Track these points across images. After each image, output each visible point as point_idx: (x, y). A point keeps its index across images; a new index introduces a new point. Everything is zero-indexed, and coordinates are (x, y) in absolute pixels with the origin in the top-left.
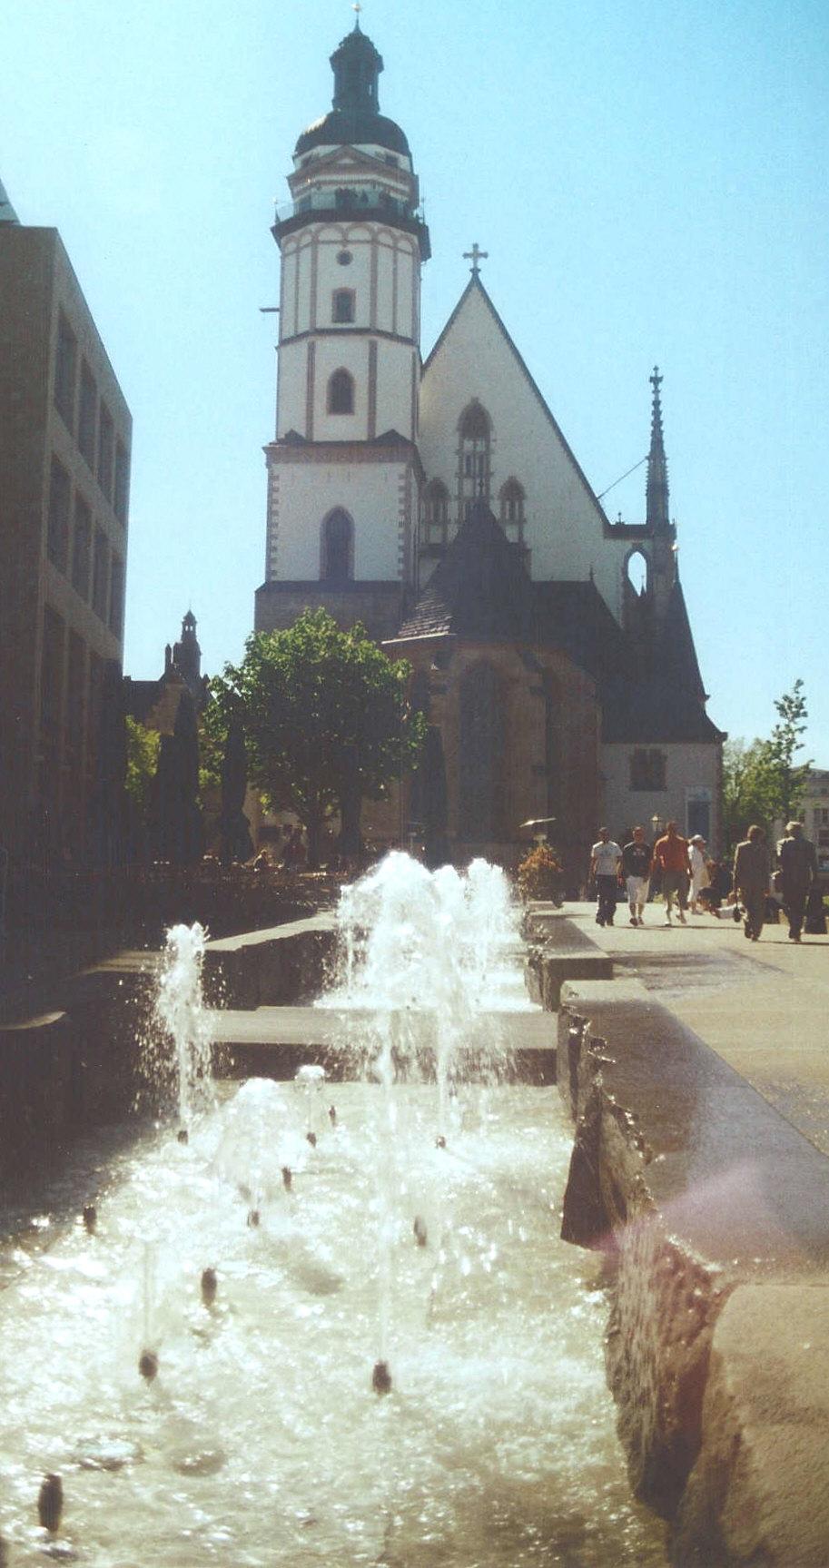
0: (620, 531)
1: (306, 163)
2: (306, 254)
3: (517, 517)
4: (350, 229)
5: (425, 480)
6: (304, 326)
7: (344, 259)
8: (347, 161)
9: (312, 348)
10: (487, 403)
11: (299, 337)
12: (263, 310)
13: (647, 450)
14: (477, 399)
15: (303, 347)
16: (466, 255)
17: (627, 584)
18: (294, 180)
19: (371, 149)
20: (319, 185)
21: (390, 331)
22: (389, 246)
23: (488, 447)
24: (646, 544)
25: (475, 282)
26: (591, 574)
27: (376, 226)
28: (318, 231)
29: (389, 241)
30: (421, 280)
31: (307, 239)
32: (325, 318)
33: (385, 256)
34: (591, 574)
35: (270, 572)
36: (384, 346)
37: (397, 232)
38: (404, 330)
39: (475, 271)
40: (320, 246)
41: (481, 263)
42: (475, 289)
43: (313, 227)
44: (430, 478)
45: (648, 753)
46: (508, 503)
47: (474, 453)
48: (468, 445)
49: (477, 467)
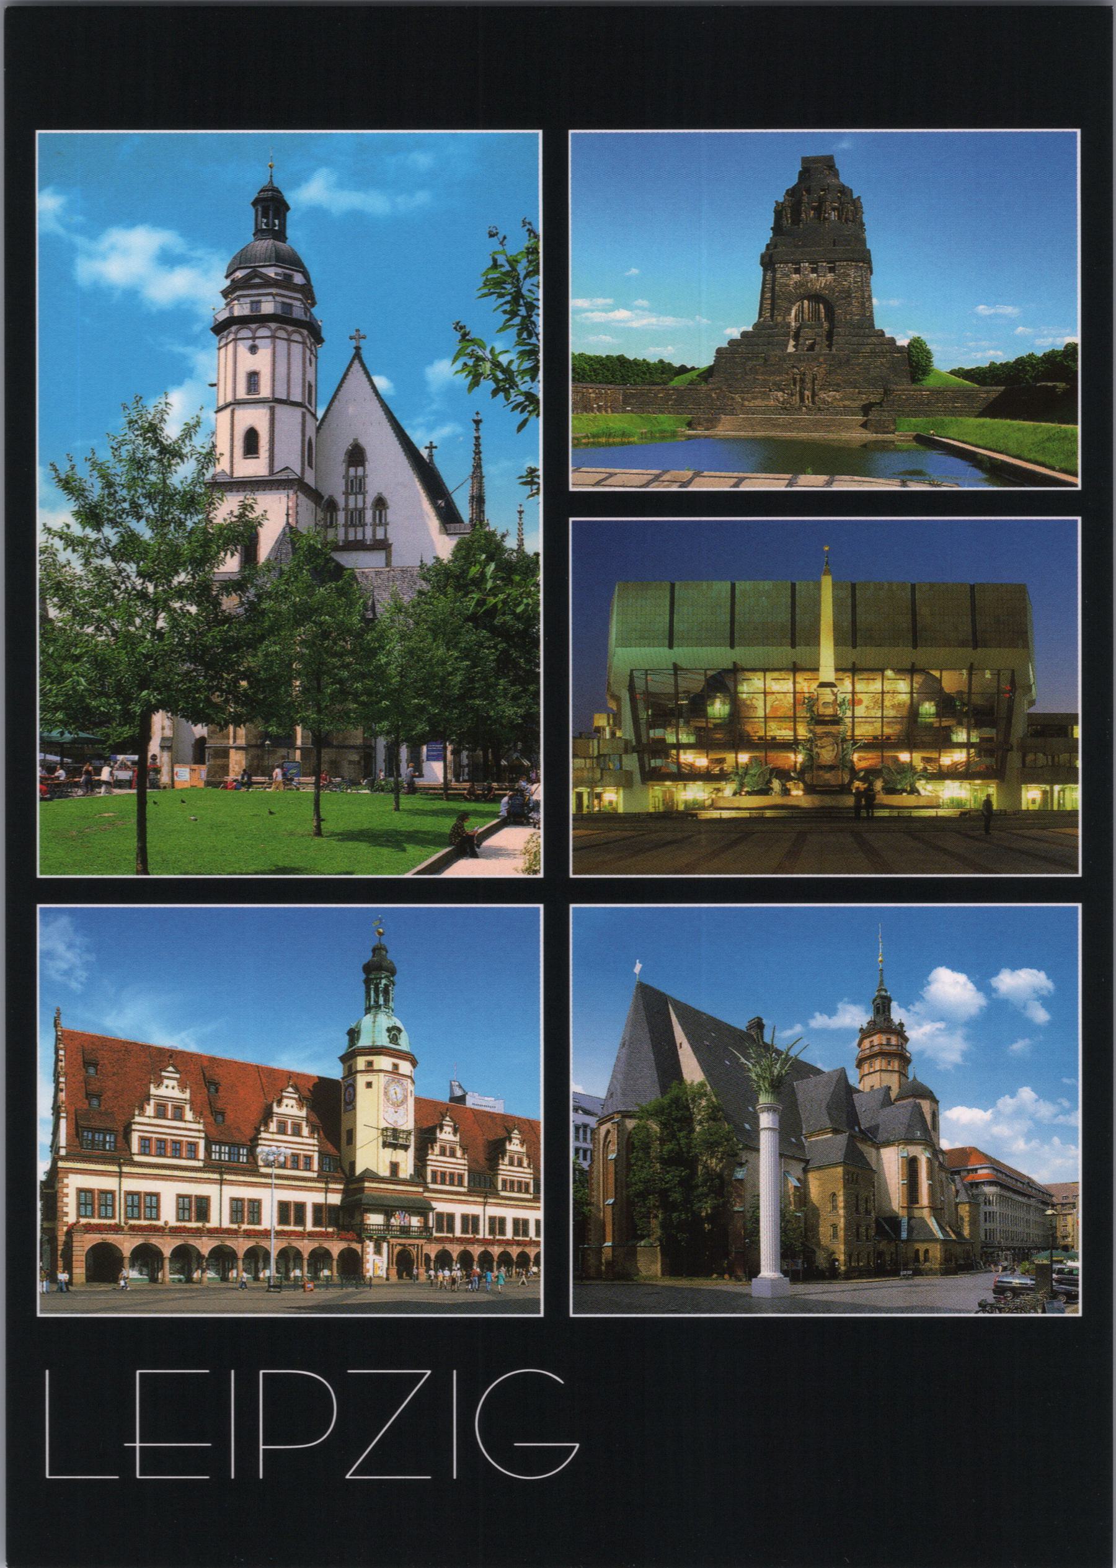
1: (233, 281)
2: (231, 346)
3: (383, 521)
4: (257, 329)
5: (322, 497)
6: (230, 399)
7: (253, 349)
8: (257, 280)
10: (363, 442)
11: (227, 406)
13: (471, 470)
15: (228, 411)
18: (225, 294)
19: (271, 272)
20: (238, 298)
21: (285, 398)
22: (283, 339)
25: (358, 355)
27: (273, 325)
28: (236, 333)
29: (284, 335)
30: (316, 357)
31: (232, 337)
32: (242, 394)
33: (282, 345)
36: (280, 410)
37: (290, 328)
38: (297, 397)
40: (239, 343)
43: (234, 328)
44: (326, 497)
46: (377, 512)
47: (356, 477)
48: (352, 470)
49: (356, 486)
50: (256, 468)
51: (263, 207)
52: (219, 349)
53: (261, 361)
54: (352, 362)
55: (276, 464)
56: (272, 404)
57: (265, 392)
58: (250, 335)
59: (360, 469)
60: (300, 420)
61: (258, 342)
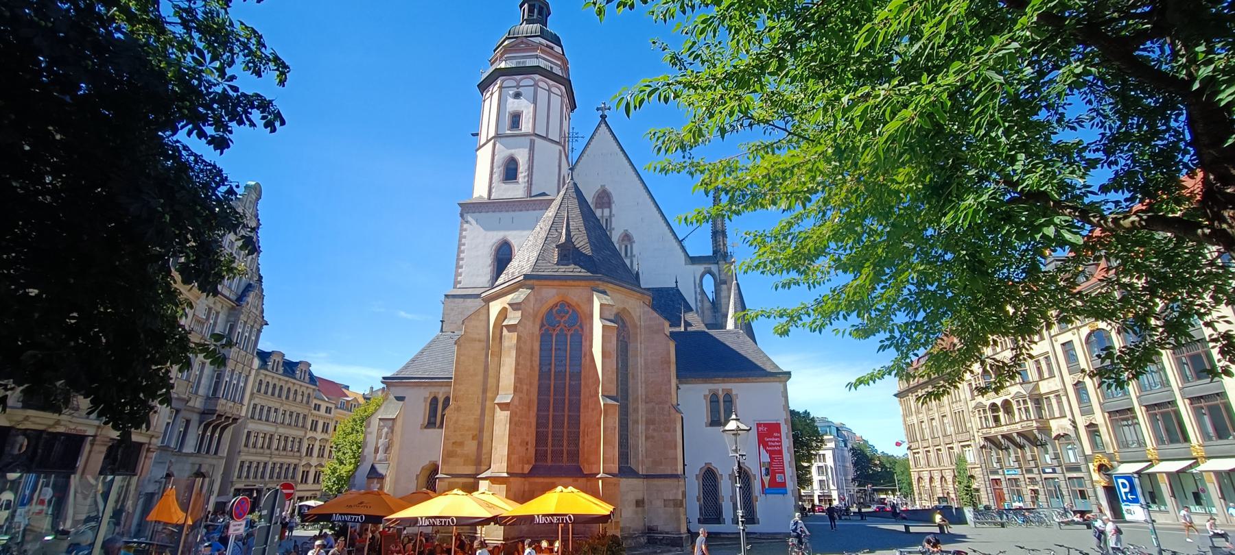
0: (694, 260)
4: (521, 80)
9: (494, 145)
10: (609, 188)
11: (488, 141)
12: (473, 135)
14: (604, 186)
16: (598, 109)
17: (703, 292)
21: (545, 135)
23: (610, 212)
24: (714, 268)
26: (676, 282)
27: (537, 77)
34: (676, 282)
35: (456, 283)
36: (538, 140)
37: (551, 83)
39: (603, 117)
41: (606, 112)
42: (603, 125)
45: (720, 392)
50: (516, 191)
51: (529, 6)
52: (484, 101)
53: (524, 106)
54: (599, 126)
55: (534, 188)
56: (533, 138)
57: (526, 126)
58: (515, 84)
59: (606, 212)
60: (558, 156)
61: (520, 90)
